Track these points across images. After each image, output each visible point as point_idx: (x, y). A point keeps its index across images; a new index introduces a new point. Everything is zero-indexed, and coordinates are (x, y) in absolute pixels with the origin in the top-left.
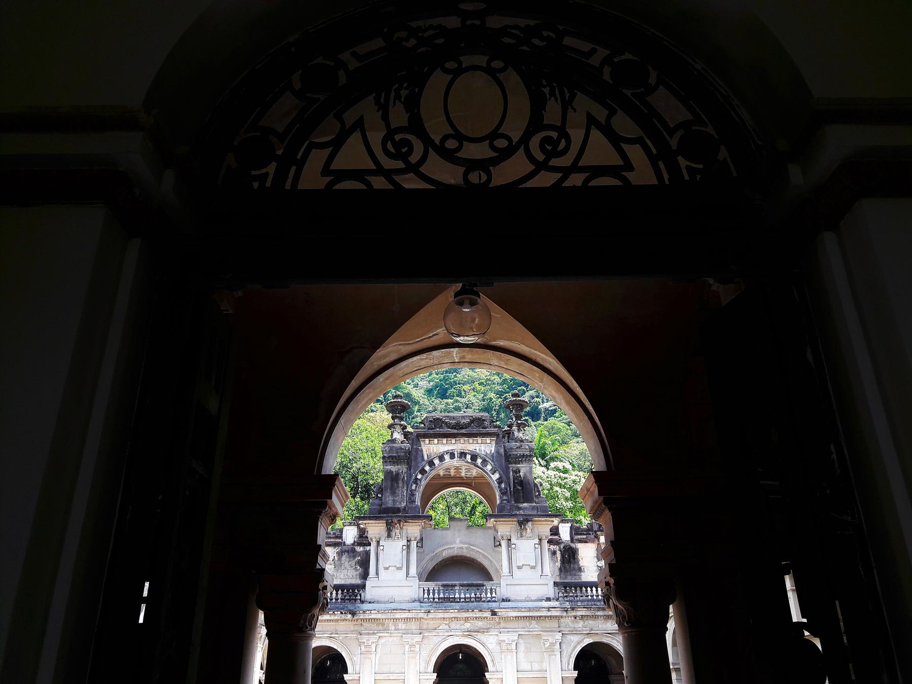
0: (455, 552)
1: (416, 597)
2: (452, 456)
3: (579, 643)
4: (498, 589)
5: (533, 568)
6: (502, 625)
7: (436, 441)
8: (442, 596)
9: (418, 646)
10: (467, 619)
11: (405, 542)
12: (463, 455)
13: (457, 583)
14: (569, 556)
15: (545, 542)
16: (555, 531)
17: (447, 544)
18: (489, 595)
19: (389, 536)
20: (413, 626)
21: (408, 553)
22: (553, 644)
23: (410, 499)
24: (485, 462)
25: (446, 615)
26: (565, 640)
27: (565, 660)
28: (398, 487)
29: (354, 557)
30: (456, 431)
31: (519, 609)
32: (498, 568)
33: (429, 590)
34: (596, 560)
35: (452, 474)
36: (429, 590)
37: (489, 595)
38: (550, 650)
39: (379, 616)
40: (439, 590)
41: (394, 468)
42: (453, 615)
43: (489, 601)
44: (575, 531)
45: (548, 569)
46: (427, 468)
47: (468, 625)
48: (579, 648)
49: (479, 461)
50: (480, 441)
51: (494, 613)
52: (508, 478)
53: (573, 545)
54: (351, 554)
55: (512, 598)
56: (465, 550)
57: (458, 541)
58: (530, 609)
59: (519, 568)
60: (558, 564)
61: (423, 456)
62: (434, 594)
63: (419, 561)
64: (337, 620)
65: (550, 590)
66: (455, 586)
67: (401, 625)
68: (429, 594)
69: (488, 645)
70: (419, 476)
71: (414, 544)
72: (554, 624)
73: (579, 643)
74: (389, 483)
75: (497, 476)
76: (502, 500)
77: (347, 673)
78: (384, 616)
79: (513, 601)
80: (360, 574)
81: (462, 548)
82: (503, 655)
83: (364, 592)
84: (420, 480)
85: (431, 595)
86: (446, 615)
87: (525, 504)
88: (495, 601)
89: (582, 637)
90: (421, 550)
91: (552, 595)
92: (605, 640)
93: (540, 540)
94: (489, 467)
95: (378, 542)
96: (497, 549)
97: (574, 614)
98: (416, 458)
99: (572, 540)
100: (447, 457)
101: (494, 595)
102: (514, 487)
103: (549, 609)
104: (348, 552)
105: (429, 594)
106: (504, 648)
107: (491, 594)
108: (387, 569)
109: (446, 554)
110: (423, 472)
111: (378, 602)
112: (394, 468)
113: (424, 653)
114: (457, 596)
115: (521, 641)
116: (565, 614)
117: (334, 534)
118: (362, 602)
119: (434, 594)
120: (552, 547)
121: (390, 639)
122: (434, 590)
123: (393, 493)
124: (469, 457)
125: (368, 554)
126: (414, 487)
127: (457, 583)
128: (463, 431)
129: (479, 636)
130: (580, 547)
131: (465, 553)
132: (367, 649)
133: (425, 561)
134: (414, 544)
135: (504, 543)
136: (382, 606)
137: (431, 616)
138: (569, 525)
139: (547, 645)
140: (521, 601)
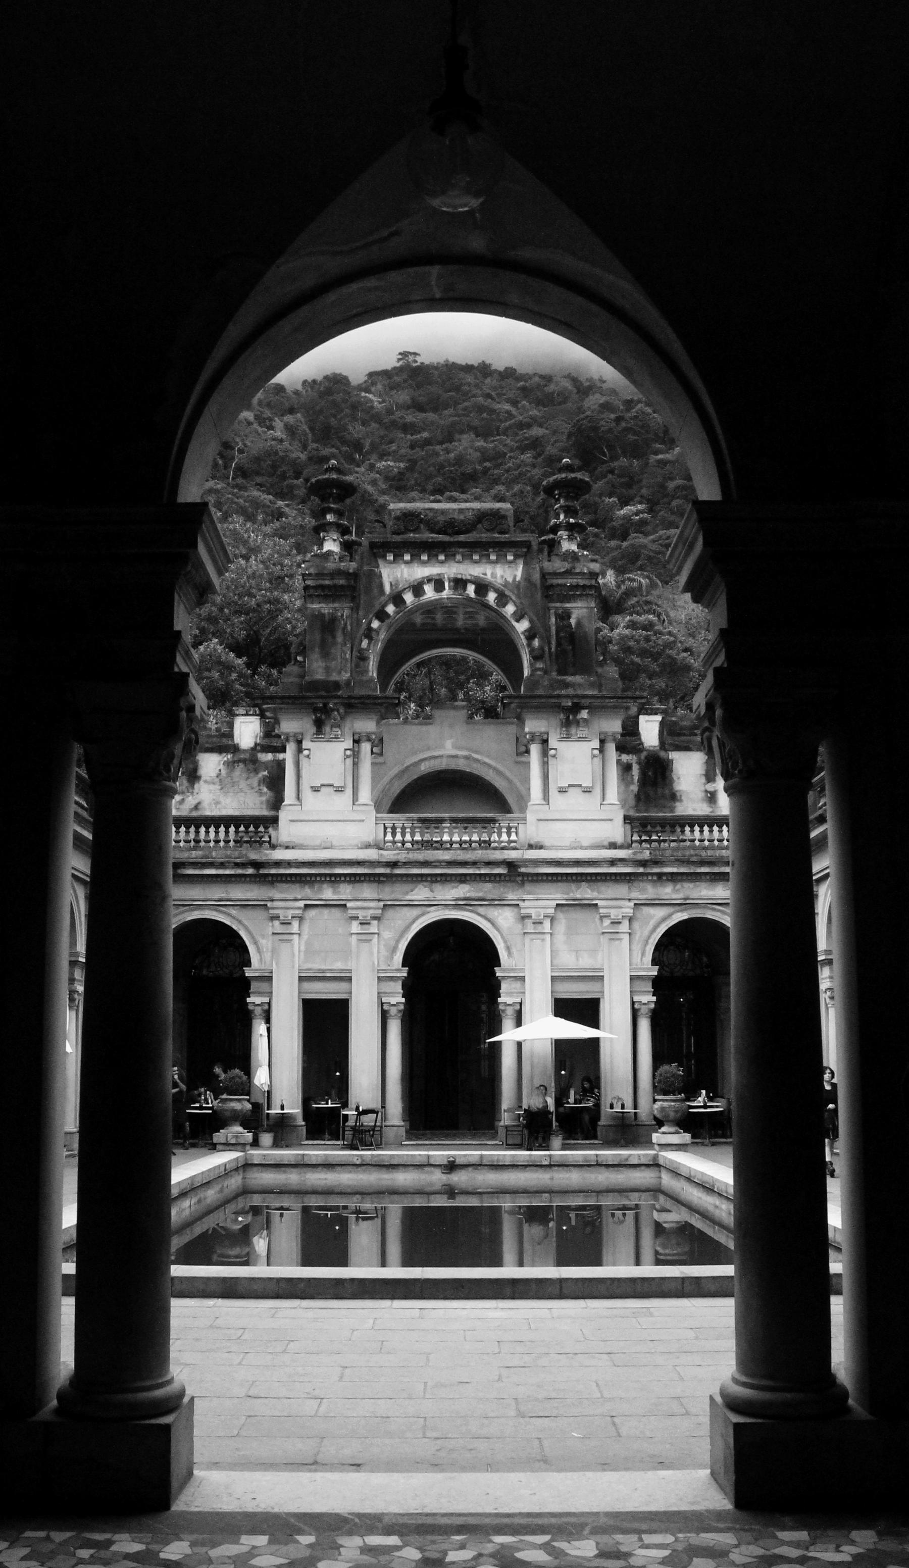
0: (442, 764)
1: (370, 839)
2: (439, 585)
3: (664, 919)
4: (521, 827)
5: (588, 791)
8: (418, 837)
10: (463, 879)
11: (349, 743)
12: (459, 583)
13: (447, 815)
14: (655, 773)
15: (611, 747)
16: (631, 730)
17: (429, 749)
18: (504, 837)
20: (368, 891)
21: (355, 765)
23: (357, 666)
24: (502, 599)
26: (638, 915)
27: (637, 948)
28: (335, 643)
29: (256, 771)
30: (446, 538)
32: (524, 792)
33: (394, 829)
34: (703, 780)
36: (394, 829)
37: (504, 837)
40: (413, 829)
41: (325, 608)
43: (503, 848)
44: (668, 731)
45: (613, 795)
46: (390, 609)
49: (491, 597)
50: (493, 557)
52: (548, 629)
53: (662, 754)
54: (251, 766)
55: (547, 843)
57: (449, 744)
58: (577, 863)
59: (562, 791)
60: (635, 788)
61: (381, 586)
62: (403, 835)
63: (375, 779)
65: (617, 831)
66: (442, 821)
67: (345, 891)
68: (394, 834)
69: (498, 924)
70: (375, 624)
71: (366, 747)
72: (621, 890)
73: (664, 919)
74: (318, 637)
75: (522, 626)
76: (534, 670)
77: (248, 963)
78: (313, 871)
80: (268, 801)
81: (456, 757)
82: (528, 937)
83: (276, 829)
84: (377, 631)
85: (399, 837)
87: (578, 679)
88: (515, 849)
90: (380, 760)
91: (619, 838)
92: (710, 915)
93: (602, 742)
94: (510, 609)
95: (299, 742)
96: (523, 759)
97: (656, 870)
98: (368, 590)
99: (662, 744)
102: (559, 644)
103: (613, 862)
104: (244, 761)
105: (394, 834)
108: (316, 790)
109: (425, 768)
110: (382, 615)
112: (325, 608)
113: (387, 935)
114: (446, 838)
115: (560, 915)
116: (641, 870)
117: (218, 730)
118: (273, 847)
119: (403, 835)
120: (625, 758)
121: (326, 911)
122: (403, 829)
123: (326, 654)
124: (471, 590)
125: (280, 766)
126: (365, 643)
127: (447, 815)
128: (462, 538)
130: (674, 755)
132: (285, 926)
133: (386, 779)
134: (366, 747)
135: (535, 749)
137: (398, 871)
138: (659, 718)
139: (607, 922)
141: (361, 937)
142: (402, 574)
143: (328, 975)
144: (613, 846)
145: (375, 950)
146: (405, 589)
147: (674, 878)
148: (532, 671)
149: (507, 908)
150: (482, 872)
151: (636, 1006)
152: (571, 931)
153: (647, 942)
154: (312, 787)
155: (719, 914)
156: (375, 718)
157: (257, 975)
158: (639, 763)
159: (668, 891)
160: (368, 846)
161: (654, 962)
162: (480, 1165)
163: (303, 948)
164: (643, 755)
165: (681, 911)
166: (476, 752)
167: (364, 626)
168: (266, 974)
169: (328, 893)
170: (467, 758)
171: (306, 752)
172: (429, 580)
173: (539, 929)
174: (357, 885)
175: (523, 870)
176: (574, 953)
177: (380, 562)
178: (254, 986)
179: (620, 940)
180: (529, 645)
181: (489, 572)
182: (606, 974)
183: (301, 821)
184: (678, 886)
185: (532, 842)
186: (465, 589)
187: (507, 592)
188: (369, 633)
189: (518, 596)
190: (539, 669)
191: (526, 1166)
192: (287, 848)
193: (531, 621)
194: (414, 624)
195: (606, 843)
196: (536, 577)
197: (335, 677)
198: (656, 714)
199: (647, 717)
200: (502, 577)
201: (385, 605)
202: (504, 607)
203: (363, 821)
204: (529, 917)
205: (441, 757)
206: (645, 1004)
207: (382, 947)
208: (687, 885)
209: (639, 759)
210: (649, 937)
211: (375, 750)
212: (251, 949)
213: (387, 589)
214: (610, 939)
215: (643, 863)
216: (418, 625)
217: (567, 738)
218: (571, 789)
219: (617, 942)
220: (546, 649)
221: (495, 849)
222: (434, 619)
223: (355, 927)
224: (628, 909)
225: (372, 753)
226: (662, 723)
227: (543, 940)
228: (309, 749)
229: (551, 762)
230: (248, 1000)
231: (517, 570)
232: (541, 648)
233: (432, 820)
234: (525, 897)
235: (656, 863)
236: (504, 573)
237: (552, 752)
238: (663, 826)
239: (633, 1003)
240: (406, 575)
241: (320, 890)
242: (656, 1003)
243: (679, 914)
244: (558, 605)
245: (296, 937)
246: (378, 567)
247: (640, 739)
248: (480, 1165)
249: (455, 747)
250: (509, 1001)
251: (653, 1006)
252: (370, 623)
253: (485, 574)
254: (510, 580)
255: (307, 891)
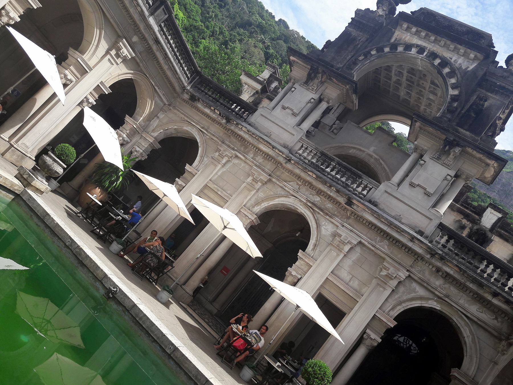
1: (290, 145)
3: (421, 298)
5: (428, 194)
6: (350, 221)
7: (414, 30)
8: (314, 161)
9: (260, 184)
10: (319, 192)
11: (316, 96)
12: (433, 55)
18: (360, 189)
19: (306, 83)
22: (389, 277)
25: (303, 175)
31: (379, 217)
35: (412, 101)
38: (383, 282)
39: (246, 136)
42: (308, 179)
43: (356, 194)
46: (387, 50)
47: (317, 199)
48: (417, 304)
49: (446, 70)
50: (462, 51)
51: (349, 203)
52: (467, 101)
53: (489, 234)
55: (382, 206)
56: (372, 160)
57: (372, 149)
59: (412, 185)
61: (391, 38)
64: (213, 120)
67: (260, 159)
68: (304, 152)
73: (421, 298)
77: (191, 164)
79: (380, 209)
81: (371, 156)
86: (303, 175)
89: (431, 296)
90: (334, 136)
92: (456, 319)
94: (453, 81)
97: (439, 264)
100: (414, 51)
101: (365, 192)
102: (468, 110)
106: (336, 242)
107: (363, 189)
110: (380, 50)
111: (256, 129)
113: (261, 194)
115: (358, 249)
116: (428, 256)
121: (243, 164)
124: (437, 62)
129: (321, 216)
130: (496, 239)
131: (371, 161)
132: (219, 158)
134: (324, 106)
136: (258, 133)
137: (289, 166)
138: (500, 215)
139: (384, 273)
140: (388, 214)
141: (249, 187)
142: (405, 38)
143: (219, 193)
144: (421, 233)
145: (249, 197)
146: (401, 44)
147: (447, 276)
148: (442, 116)
149: (331, 225)
150: (331, 194)
151: (365, 336)
152: (358, 263)
153: (400, 303)
154: (283, 106)
155: (463, 323)
156: (338, 92)
157: (190, 170)
158: (471, 229)
159: (437, 282)
160: (285, 147)
161: (395, 319)
162: (128, 311)
163: (219, 173)
164: (475, 227)
165: (436, 301)
166: (383, 160)
167: (367, 50)
168: (194, 173)
169: (250, 156)
170: (376, 159)
171: (293, 89)
172: (417, 46)
173: (341, 246)
174: (266, 161)
175: (355, 207)
176: (351, 276)
177: (399, 27)
178: (185, 175)
179: (384, 289)
180: (449, 103)
181: (454, 59)
182: (360, 301)
183: (266, 118)
184: (447, 286)
185: (373, 200)
186: (434, 59)
187: (457, 72)
188: (367, 55)
189: (462, 77)
190: (447, 117)
191: (155, 341)
192: (249, 124)
193: (460, 92)
194: (399, 97)
195: (417, 229)
196: (481, 73)
197: (334, 63)
198: (499, 212)
199: (493, 211)
200: (460, 64)
201: (386, 46)
202: (450, 78)
203: (294, 135)
204: (340, 236)
205: (364, 151)
206: (371, 339)
207: (253, 200)
208: (452, 288)
209: (473, 227)
210: (404, 301)
211: (335, 131)
212: (198, 158)
213: (393, 40)
214: (378, 284)
215: (433, 254)
216: (401, 98)
217: (438, 159)
218: (418, 188)
219: (381, 289)
220: (459, 110)
221: (349, 191)
222: (410, 97)
223: (250, 179)
224: (403, 274)
225: (333, 132)
226: (499, 219)
227: (338, 255)
228: (295, 89)
229: (417, 167)
230: (177, 179)
231: (472, 65)
232: (456, 108)
233: (328, 157)
234: (345, 224)
235: (442, 259)
236: (464, 61)
237: (422, 162)
238: (462, 247)
239: (364, 332)
240: (407, 39)
241: (248, 152)
242: (379, 344)
243: (435, 303)
244: (484, 91)
245: (220, 166)
246: (395, 29)
247: (481, 219)
248: (128, 311)
249: (374, 152)
250: (294, 273)
251: (376, 344)
252: (371, 50)
253: (451, 59)
254: (464, 67)
255: (242, 149)
